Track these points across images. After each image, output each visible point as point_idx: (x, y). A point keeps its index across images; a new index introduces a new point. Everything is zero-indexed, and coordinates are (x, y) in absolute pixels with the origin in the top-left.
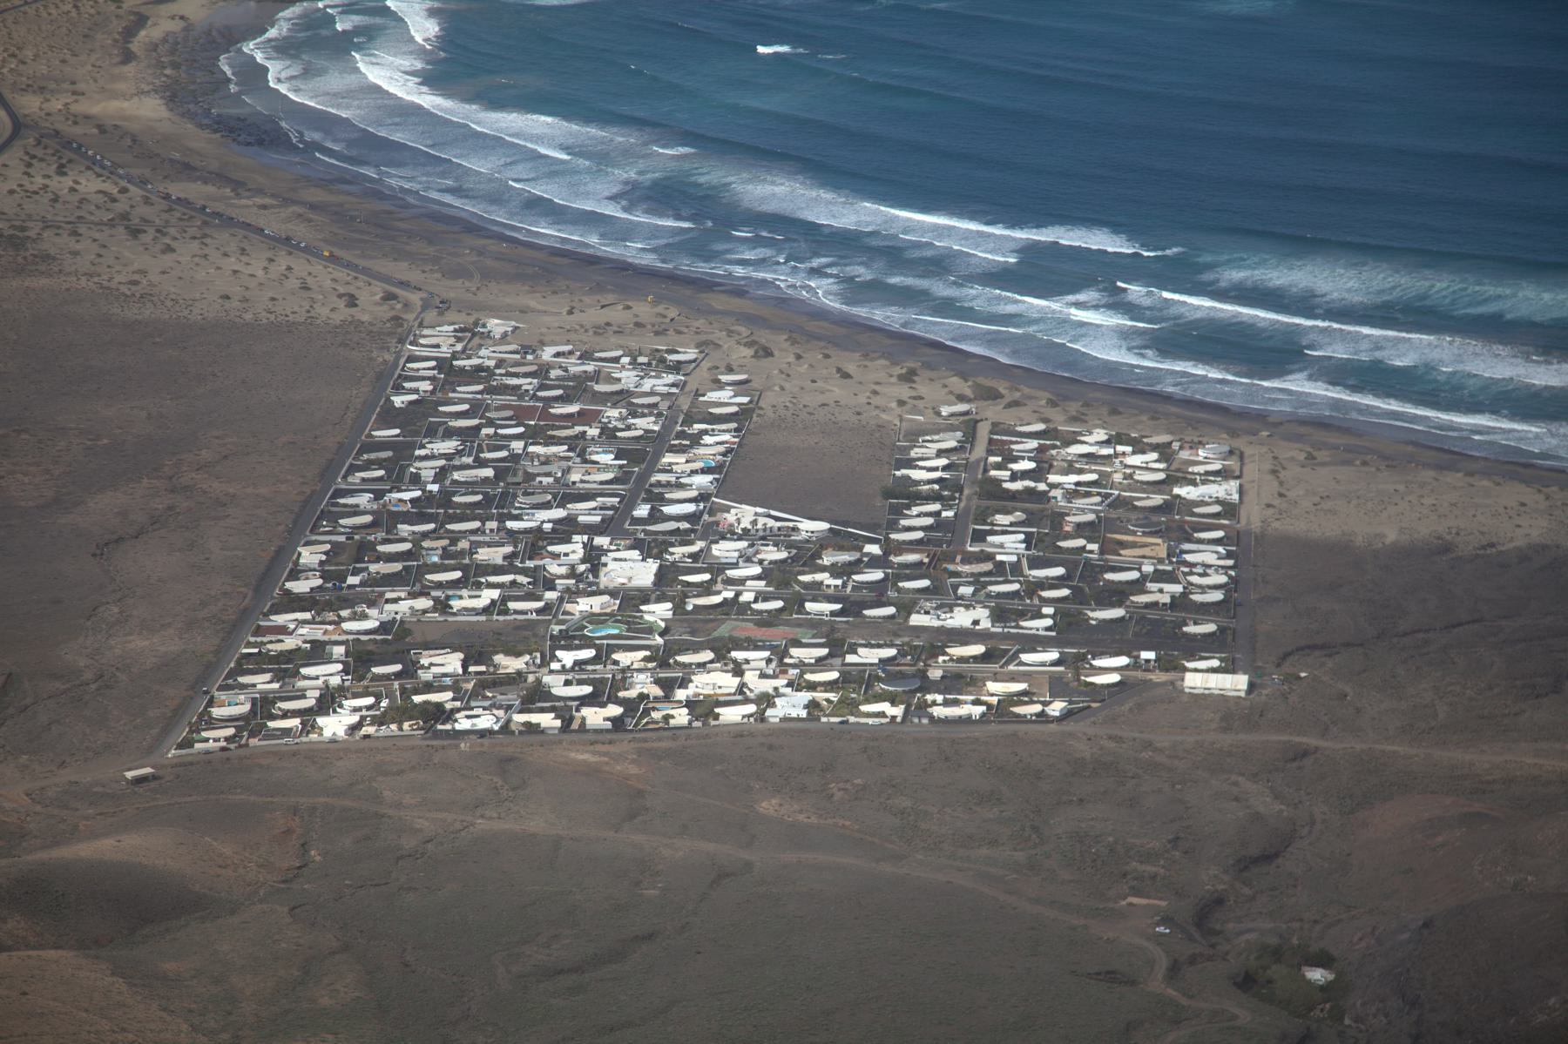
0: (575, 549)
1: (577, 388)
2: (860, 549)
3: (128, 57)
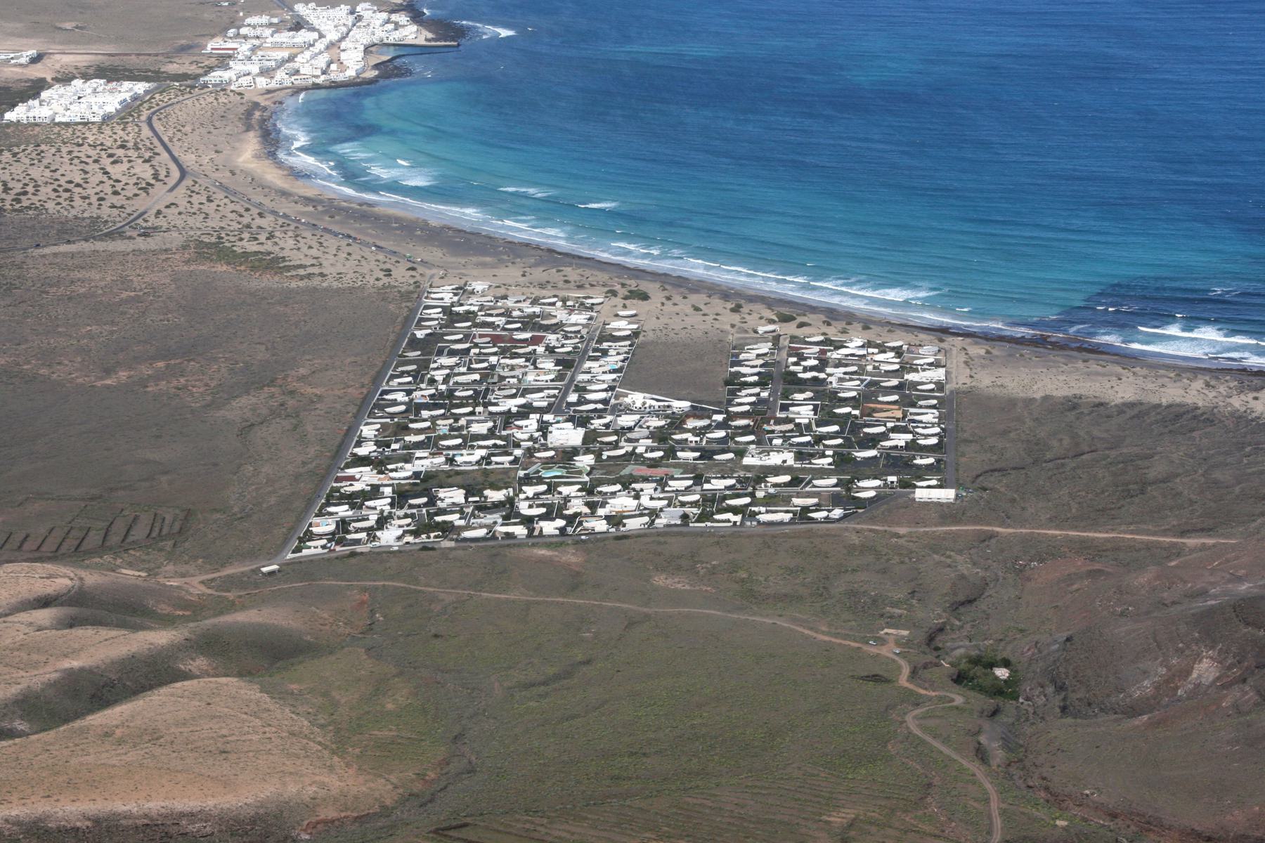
0: (532, 423)
1: (529, 322)
2: (710, 418)
3: (249, 128)
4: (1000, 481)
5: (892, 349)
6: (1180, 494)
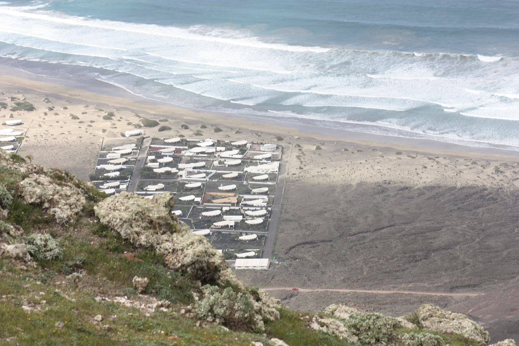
4: (309, 252)
5: (238, 147)
6: (456, 258)
